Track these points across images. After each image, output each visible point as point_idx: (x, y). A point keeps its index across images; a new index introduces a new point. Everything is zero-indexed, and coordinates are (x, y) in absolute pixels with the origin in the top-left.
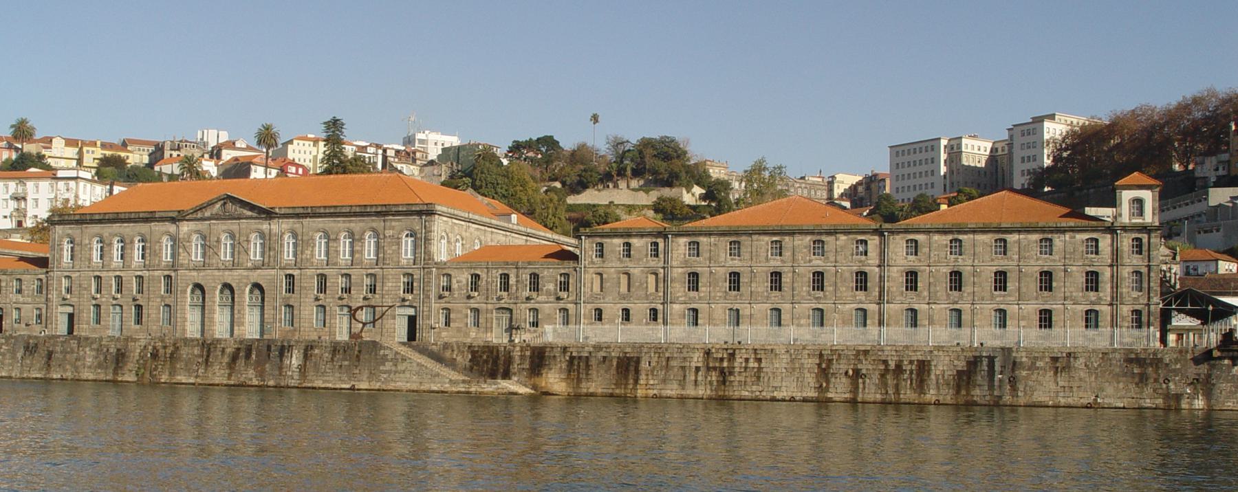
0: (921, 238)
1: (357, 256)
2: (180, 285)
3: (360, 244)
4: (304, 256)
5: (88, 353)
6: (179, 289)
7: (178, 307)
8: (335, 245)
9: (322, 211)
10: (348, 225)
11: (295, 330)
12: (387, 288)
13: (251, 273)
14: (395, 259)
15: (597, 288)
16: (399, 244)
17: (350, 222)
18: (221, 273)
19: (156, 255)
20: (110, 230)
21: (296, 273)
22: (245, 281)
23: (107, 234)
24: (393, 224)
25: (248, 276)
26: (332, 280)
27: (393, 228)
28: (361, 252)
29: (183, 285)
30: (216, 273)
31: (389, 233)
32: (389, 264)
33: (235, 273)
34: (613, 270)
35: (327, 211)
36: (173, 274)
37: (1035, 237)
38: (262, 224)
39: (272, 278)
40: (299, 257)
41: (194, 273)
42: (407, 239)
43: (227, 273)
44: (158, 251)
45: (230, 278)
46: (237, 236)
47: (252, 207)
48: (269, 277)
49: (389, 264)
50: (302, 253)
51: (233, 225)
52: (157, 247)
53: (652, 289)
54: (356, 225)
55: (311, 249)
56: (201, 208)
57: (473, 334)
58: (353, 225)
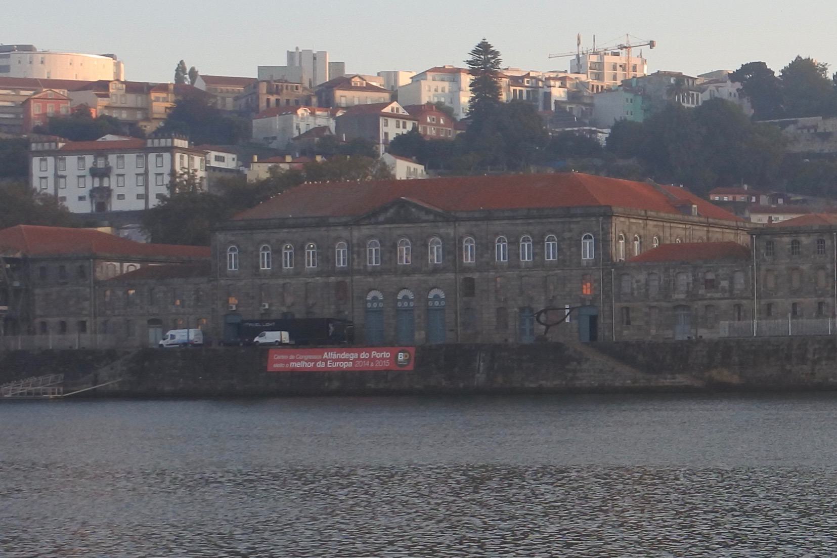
16: (579, 246)
17: (530, 224)
21: (476, 276)
24: (572, 226)
27: (570, 231)
31: (567, 235)
36: (348, 280)
42: (585, 241)
56: (375, 214)
57: (653, 332)
58: (531, 228)
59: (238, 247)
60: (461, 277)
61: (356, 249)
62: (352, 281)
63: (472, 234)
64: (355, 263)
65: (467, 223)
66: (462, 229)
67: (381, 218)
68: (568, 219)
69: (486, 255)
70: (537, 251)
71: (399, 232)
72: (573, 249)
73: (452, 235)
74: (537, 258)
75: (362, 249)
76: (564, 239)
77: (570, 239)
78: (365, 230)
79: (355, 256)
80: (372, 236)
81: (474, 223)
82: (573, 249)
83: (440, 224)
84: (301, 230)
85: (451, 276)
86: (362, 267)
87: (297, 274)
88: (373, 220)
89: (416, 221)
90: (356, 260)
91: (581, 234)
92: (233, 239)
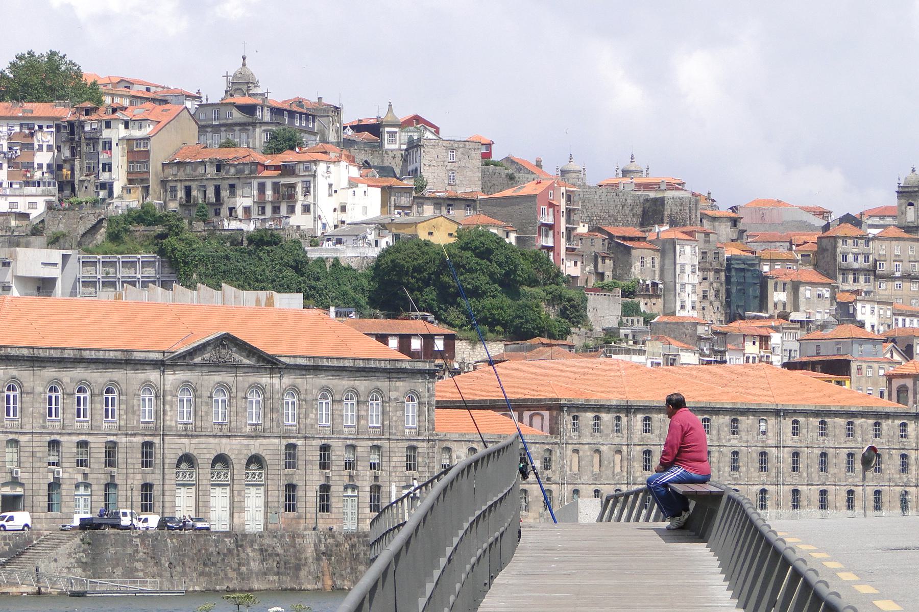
0: (801, 420)
1: (362, 422)
4: (309, 421)
6: (167, 461)
9: (325, 363)
11: (300, 517)
13: (251, 441)
15: (575, 469)
19: (134, 412)
21: (299, 442)
22: (245, 452)
23: (69, 381)
27: (396, 389)
31: (393, 395)
32: (395, 434)
34: (587, 447)
35: (330, 364)
36: (157, 440)
37: (871, 421)
39: (271, 448)
40: (303, 421)
41: (185, 440)
44: (136, 408)
45: (228, 447)
46: (234, 390)
47: (251, 351)
48: (272, 448)
49: (395, 434)
50: (306, 417)
52: (135, 402)
53: (618, 469)
55: (314, 412)
60: (284, 442)
61: (168, 398)
67: (197, 360)
73: (277, 387)
82: (399, 413)
85: (276, 441)
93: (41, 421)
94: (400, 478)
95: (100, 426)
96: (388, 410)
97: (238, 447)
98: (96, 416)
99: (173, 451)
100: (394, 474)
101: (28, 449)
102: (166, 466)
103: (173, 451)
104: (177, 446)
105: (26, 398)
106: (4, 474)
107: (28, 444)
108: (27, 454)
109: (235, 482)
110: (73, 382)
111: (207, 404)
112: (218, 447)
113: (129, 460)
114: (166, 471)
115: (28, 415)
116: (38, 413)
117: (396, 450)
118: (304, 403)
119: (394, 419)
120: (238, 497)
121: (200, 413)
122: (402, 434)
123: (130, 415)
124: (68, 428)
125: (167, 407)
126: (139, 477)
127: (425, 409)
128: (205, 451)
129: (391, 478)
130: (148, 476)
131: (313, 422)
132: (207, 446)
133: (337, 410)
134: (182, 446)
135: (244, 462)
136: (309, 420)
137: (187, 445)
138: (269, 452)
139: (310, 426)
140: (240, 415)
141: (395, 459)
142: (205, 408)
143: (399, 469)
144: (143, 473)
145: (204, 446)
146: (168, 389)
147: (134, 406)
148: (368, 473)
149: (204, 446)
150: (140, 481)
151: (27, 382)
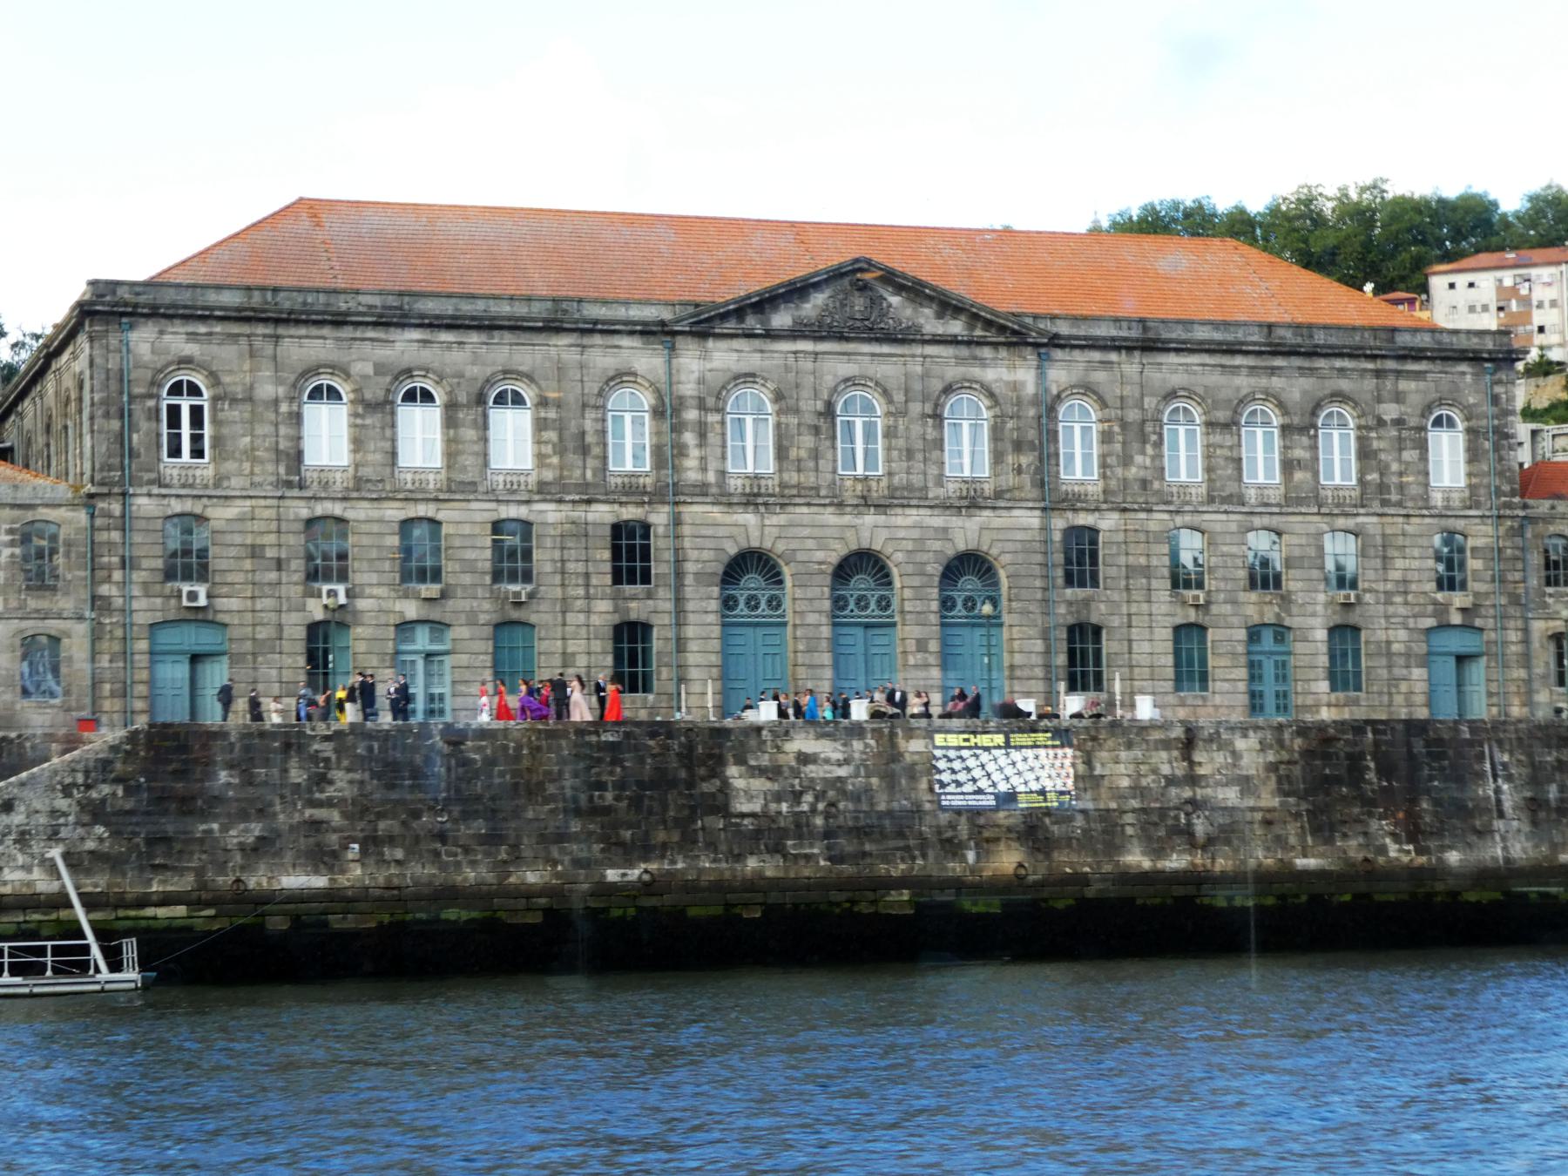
2: (693, 554)
3: (1305, 440)
5: (739, 783)
6: (690, 567)
7: (690, 632)
8: (1228, 440)
10: (1263, 382)
12: (1396, 575)
13: (955, 522)
14: (1415, 490)
17: (1273, 371)
18: (847, 519)
19: (584, 450)
20: (382, 353)
21: (1107, 523)
22: (937, 545)
24: (1404, 385)
25: (945, 530)
26: (1225, 549)
27: (1399, 398)
28: (1312, 466)
29: (706, 555)
30: (829, 517)
31: (1390, 411)
33: (900, 521)
36: (659, 518)
38: (983, 363)
41: (749, 518)
43: (870, 519)
44: (590, 439)
46: (899, 397)
47: (948, 306)
48: (1020, 536)
50: (1126, 461)
51: (888, 364)
52: (589, 425)
54: (1296, 386)
55: (1149, 450)
56: (765, 303)
58: (1277, 382)
59: (214, 378)
60: (1059, 523)
61: (691, 415)
62: (677, 521)
63: (1087, 389)
64: (691, 462)
65: (1077, 354)
66: (1061, 373)
67: (782, 319)
68: (1391, 364)
69: (1139, 459)
70: (1299, 453)
71: (846, 369)
72: (1410, 455)
73: (1030, 389)
74: (1299, 476)
75: (713, 418)
76: (1381, 423)
77: (1399, 422)
78: (724, 356)
79: (689, 438)
80: (749, 377)
81: (1096, 356)
82: (1410, 455)
83: (987, 352)
84: (474, 337)
86: (711, 477)
87: (458, 488)
88: (752, 322)
89: (905, 337)
90: (694, 453)
91: (1428, 408)
92: (191, 349)
93: (282, 470)
94: (1417, 609)
95: (474, 483)
96: (1375, 444)
97: (916, 534)
98: (461, 459)
99: (709, 543)
100: (1398, 599)
101: (238, 539)
102: (689, 580)
103: (709, 543)
104: (721, 532)
105: (230, 413)
106: (159, 601)
107: (237, 526)
108: (233, 552)
109: (908, 617)
110: (384, 374)
111: (816, 430)
112: (849, 534)
113: (571, 567)
114: (689, 591)
115: (237, 455)
116: (267, 450)
117: (1400, 541)
118: (1117, 429)
119: (1395, 467)
120: (919, 656)
121: (793, 453)
122: (1420, 504)
123: (573, 458)
124: (369, 486)
125: (689, 438)
126: (603, 606)
127: (1487, 445)
128: (810, 544)
129: (1391, 609)
130: (633, 605)
131: (1148, 475)
132: (817, 532)
133: (1221, 447)
134: (735, 530)
135: (935, 569)
136: (1134, 470)
137: (750, 529)
138: (1010, 546)
139: (1136, 487)
140: (919, 456)
141: (1399, 563)
142: (808, 441)
143: (1414, 587)
144: (614, 598)
145: (806, 532)
146: (689, 393)
147: (583, 433)
148: (1321, 597)
149: (806, 532)
150: (609, 617)
151: (231, 372)
